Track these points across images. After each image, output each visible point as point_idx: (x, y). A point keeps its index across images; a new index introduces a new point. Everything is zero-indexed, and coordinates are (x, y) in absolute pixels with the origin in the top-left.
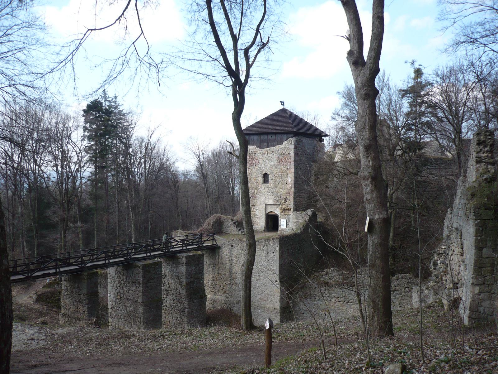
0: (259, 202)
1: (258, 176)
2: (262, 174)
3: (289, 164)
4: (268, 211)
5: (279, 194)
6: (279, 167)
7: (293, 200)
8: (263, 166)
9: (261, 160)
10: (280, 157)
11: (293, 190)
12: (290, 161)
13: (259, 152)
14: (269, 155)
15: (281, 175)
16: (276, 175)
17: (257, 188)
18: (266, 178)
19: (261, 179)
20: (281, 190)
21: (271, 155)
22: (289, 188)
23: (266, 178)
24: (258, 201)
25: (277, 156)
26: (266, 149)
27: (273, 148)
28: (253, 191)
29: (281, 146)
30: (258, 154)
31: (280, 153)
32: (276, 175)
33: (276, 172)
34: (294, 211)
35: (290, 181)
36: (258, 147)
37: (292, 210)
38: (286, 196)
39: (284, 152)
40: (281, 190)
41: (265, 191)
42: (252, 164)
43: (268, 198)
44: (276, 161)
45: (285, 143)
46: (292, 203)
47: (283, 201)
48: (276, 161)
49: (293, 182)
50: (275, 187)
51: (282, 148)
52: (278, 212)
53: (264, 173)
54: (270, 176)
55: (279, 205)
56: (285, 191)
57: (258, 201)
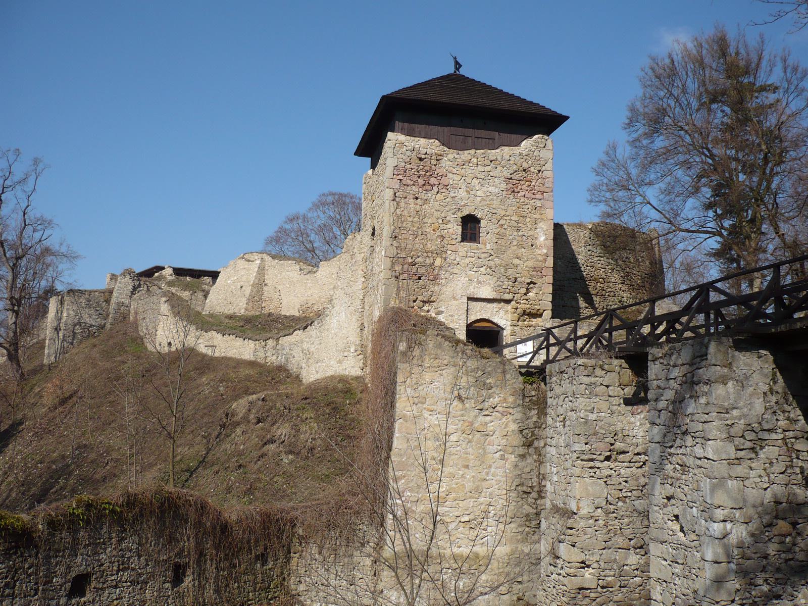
0: (447, 291)
1: (445, 221)
2: (460, 215)
3: (539, 196)
4: (472, 318)
5: (510, 272)
6: (511, 200)
7: (550, 289)
8: (462, 193)
9: (457, 178)
10: (514, 176)
11: (550, 262)
12: (542, 189)
13: (450, 156)
14: (480, 168)
15: (518, 222)
16: (502, 222)
17: (441, 252)
18: (470, 227)
19: (456, 230)
20: (516, 261)
21: (487, 169)
22: (540, 258)
23: (470, 227)
24: (444, 289)
25: (507, 173)
26: (472, 151)
27: (493, 153)
28: (428, 261)
29: (516, 150)
30: (445, 163)
31: (515, 167)
32: (502, 222)
33: (503, 213)
34: (553, 317)
35: (542, 238)
36: (443, 145)
37: (548, 314)
38: (531, 276)
39: (525, 165)
40: (516, 261)
41: (467, 260)
42: (428, 187)
43: (479, 282)
44: (503, 186)
45: (527, 144)
46: (550, 298)
47: (523, 291)
48: (503, 186)
49: (550, 243)
50: (499, 251)
51: (520, 154)
52: (502, 317)
53: (466, 212)
54: (483, 223)
55: (508, 302)
56: (530, 263)
57: (444, 289)
